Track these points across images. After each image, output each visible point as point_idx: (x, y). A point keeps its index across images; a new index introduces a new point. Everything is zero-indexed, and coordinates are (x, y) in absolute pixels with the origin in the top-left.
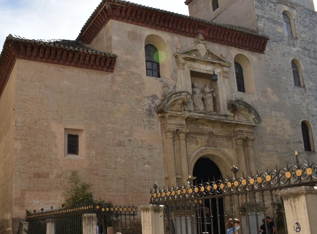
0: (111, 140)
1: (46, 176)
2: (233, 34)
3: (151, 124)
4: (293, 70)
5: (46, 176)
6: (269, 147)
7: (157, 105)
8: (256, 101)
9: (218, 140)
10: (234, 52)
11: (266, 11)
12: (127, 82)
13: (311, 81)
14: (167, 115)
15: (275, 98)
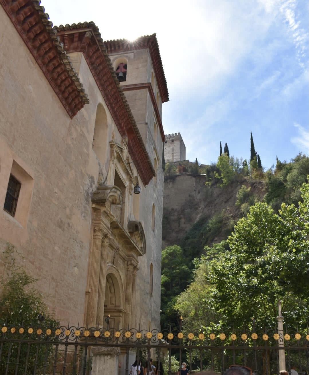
14: (103, 209)
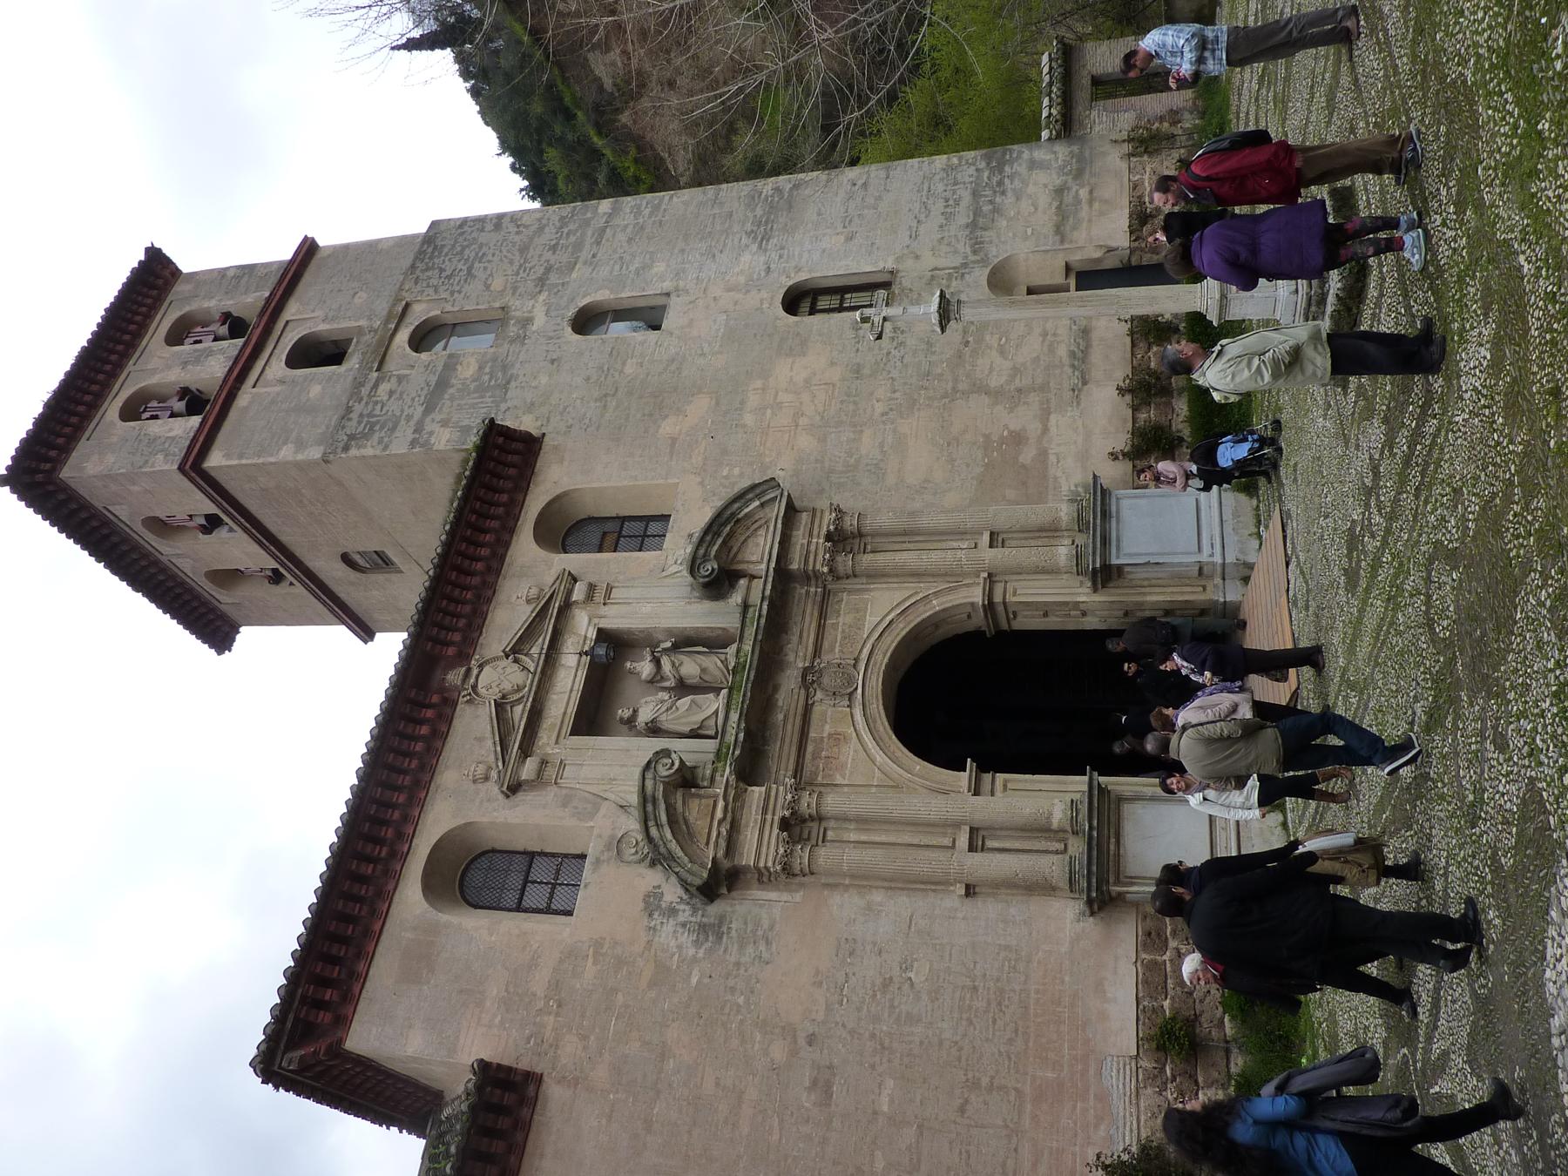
2: (460, 553)
3: (754, 932)
6: (868, 444)
7: (685, 897)
8: (701, 483)
9: (832, 650)
12: (583, 1016)
13: (650, 267)
14: (726, 864)
15: (700, 407)
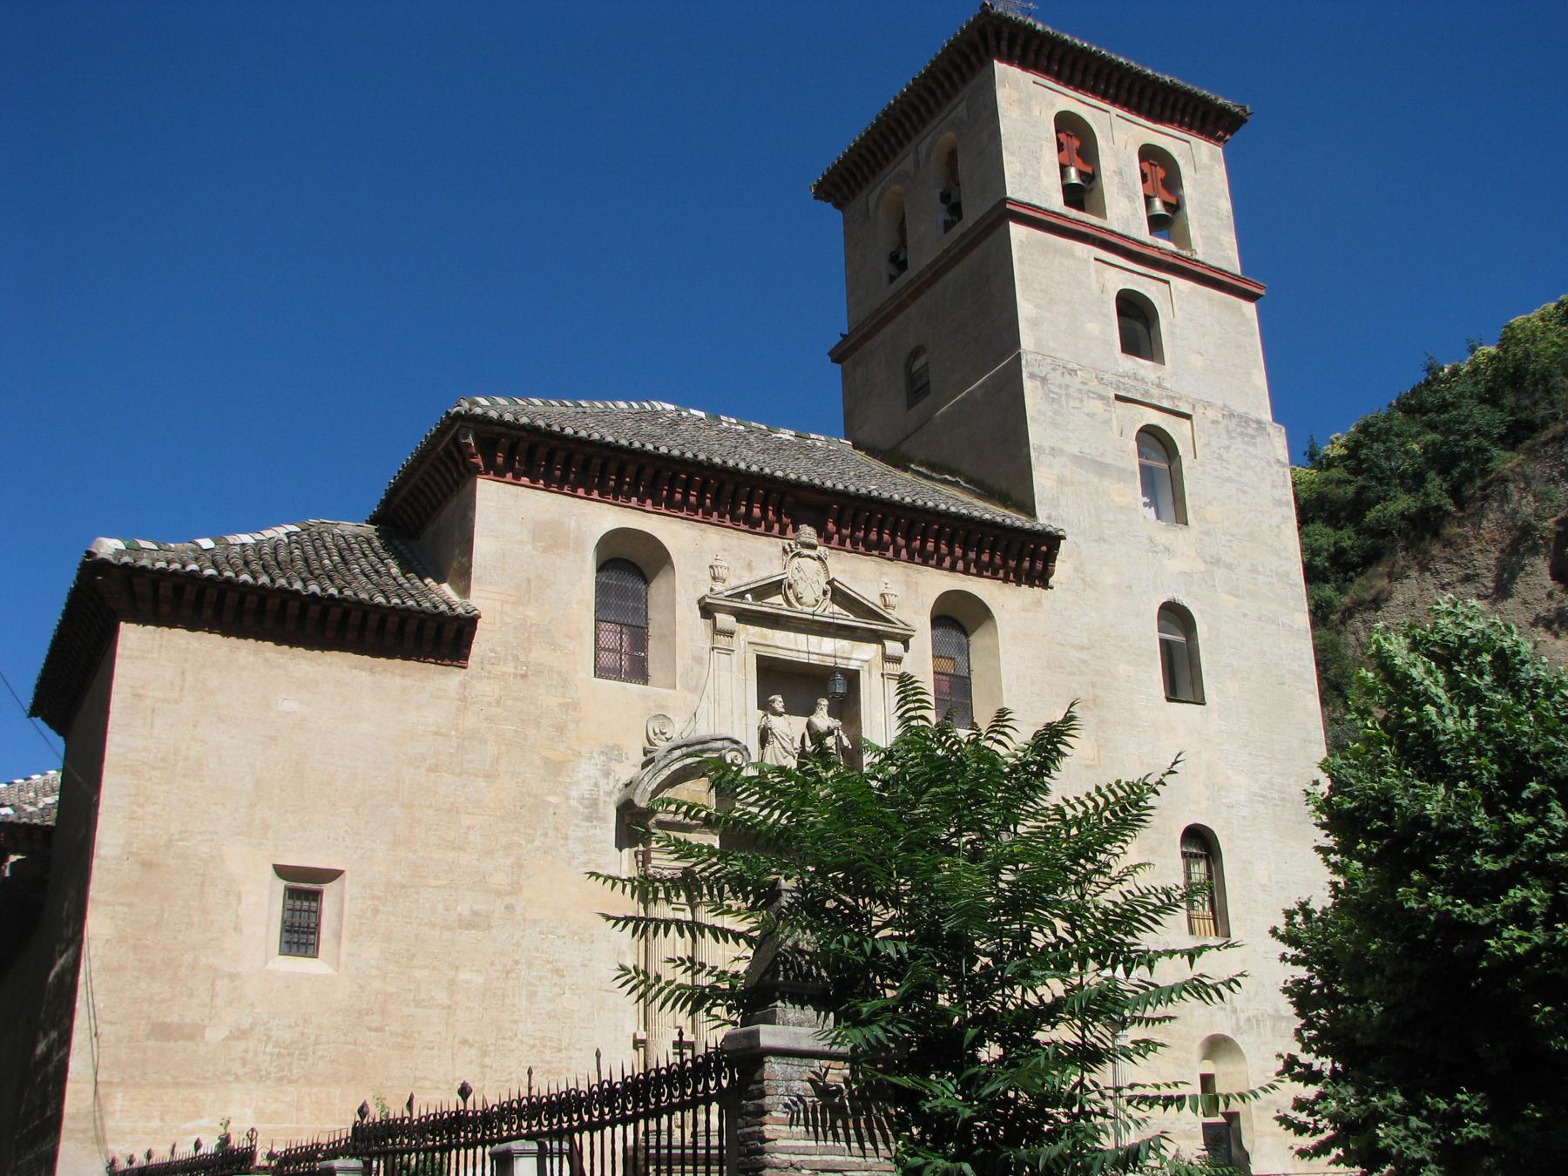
0: (440, 908)
1: (192, 1033)
4: (1162, 641)
5: (192, 1033)
10: (936, 582)
11: (1073, 431)
